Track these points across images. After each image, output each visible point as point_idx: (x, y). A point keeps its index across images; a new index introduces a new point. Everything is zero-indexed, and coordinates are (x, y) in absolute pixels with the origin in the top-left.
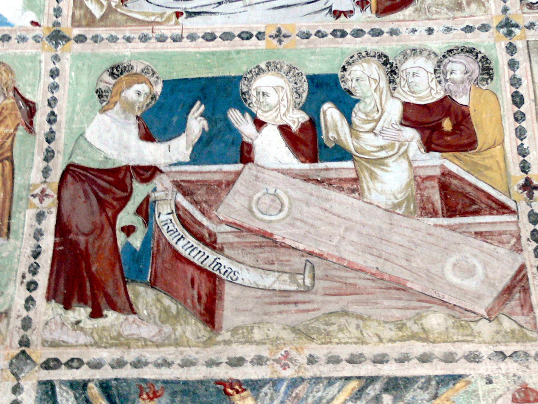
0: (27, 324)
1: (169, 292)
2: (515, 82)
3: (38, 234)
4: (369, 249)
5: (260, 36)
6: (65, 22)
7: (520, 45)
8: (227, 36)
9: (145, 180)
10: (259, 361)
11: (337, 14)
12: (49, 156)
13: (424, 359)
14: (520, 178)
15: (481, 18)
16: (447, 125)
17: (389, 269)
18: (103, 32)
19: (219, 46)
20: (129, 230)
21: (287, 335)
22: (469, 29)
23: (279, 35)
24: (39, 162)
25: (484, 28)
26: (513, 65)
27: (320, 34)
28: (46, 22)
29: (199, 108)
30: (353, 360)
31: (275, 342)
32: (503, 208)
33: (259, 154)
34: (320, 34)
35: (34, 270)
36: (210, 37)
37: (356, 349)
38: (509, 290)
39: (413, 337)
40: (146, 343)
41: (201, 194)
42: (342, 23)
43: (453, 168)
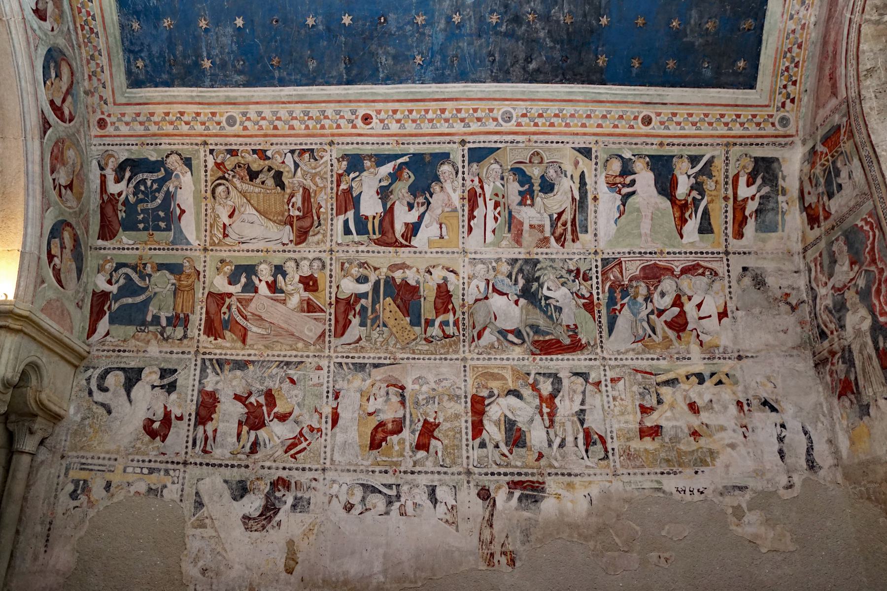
0: (198, 341)
1: (234, 333)
2: (331, 270)
3: (201, 314)
4: (286, 322)
5: (262, 251)
6: (208, 244)
7: (334, 258)
8: (253, 251)
9: (229, 298)
10: (255, 355)
11: (284, 244)
12: (204, 288)
13: (296, 356)
14: (328, 301)
15: (324, 248)
16: (311, 283)
17: (290, 328)
18: (218, 248)
19: (250, 254)
20: (225, 313)
21: (263, 348)
22: (320, 252)
23: (267, 251)
24: (201, 291)
25: (325, 251)
26: (331, 264)
27: (279, 251)
28: (202, 244)
29: (244, 275)
30: (278, 356)
31: (259, 349)
32: (323, 311)
33: (260, 292)
34: (279, 251)
35: (200, 325)
36: (248, 251)
37: (279, 353)
38: (320, 336)
39: (294, 350)
40: (228, 348)
41: (244, 303)
42: (285, 248)
43: (311, 297)
